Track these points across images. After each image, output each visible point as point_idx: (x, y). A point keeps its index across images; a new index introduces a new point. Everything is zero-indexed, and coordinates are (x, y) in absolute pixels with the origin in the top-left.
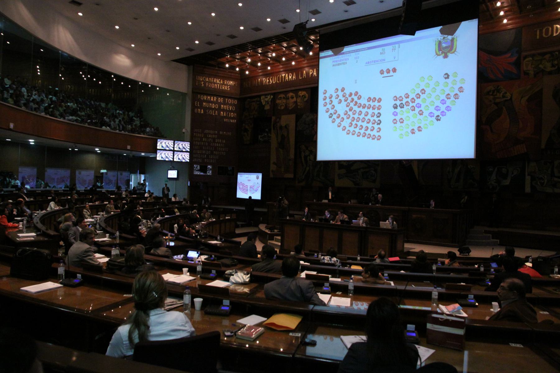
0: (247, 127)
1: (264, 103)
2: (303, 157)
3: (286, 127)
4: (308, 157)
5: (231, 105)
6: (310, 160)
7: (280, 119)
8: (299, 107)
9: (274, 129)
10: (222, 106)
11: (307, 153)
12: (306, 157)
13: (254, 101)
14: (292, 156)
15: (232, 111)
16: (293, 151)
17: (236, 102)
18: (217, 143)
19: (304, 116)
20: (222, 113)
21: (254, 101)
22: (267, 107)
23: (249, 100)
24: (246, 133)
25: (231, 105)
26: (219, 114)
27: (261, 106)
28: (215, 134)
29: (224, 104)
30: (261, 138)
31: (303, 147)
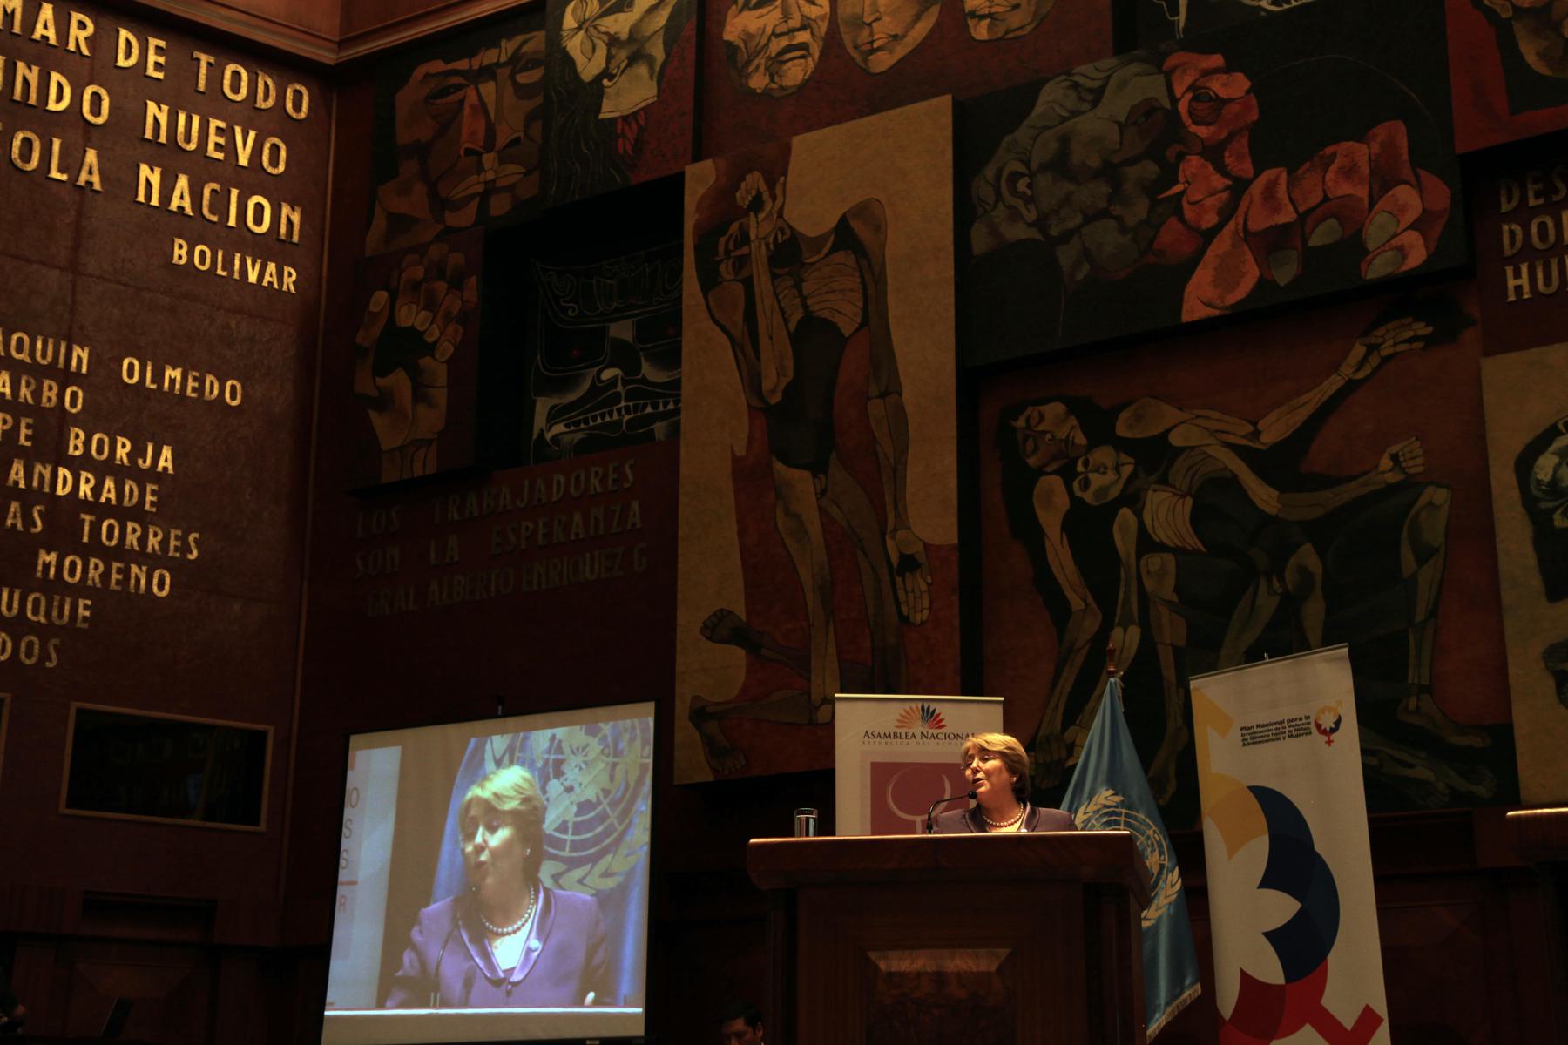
0: (410, 316)
1: (589, 67)
2: (1051, 520)
3: (844, 236)
4: (1124, 526)
5: (248, 114)
6: (1146, 543)
7: (776, 171)
8: (981, 31)
9: (709, 280)
10: (156, 112)
11: (1105, 475)
12: (1088, 526)
13: (488, 72)
14: (930, 511)
15: (253, 179)
16: (948, 461)
17: (299, 102)
18: (76, 466)
19: (1052, 96)
20: (149, 175)
21: (488, 72)
22: (631, 94)
23: (438, 66)
24: (399, 381)
25: (248, 114)
26: (121, 180)
27: (566, 97)
28: (65, 377)
29: (178, 94)
30: (554, 415)
31: (1053, 420)
